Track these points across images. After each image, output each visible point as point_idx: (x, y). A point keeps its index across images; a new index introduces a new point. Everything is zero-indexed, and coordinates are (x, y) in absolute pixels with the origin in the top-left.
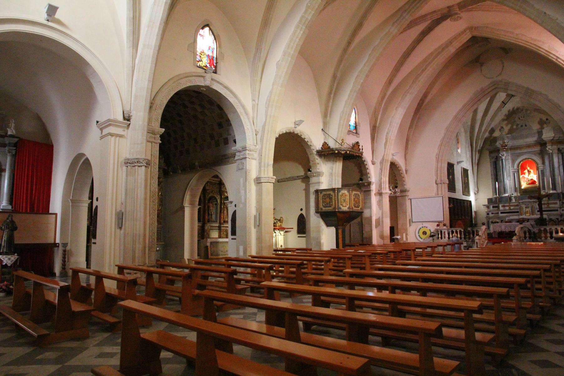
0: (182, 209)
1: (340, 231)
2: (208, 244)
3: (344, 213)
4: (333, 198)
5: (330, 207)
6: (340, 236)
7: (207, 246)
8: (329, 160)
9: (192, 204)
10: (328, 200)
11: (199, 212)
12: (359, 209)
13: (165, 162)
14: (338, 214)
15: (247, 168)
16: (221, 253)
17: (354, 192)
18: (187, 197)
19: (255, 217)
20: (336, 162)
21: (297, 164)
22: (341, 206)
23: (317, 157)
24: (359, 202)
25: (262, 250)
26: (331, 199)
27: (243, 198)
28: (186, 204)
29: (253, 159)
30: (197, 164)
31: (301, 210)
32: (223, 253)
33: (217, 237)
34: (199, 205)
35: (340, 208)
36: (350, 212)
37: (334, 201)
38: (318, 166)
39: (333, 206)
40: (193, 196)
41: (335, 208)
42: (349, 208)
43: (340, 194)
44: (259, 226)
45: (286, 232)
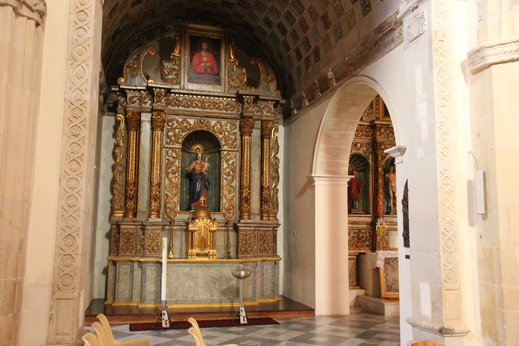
0: (310, 183)
2: (380, 264)
7: (377, 270)
9: (332, 171)
11: (349, 189)
13: (278, 88)
15: (435, 27)
18: (320, 158)
19: (471, 185)
25: (501, 304)
27: (424, 126)
28: (319, 170)
30: (330, 74)
34: (350, 173)
40: (333, 154)
44: (485, 216)
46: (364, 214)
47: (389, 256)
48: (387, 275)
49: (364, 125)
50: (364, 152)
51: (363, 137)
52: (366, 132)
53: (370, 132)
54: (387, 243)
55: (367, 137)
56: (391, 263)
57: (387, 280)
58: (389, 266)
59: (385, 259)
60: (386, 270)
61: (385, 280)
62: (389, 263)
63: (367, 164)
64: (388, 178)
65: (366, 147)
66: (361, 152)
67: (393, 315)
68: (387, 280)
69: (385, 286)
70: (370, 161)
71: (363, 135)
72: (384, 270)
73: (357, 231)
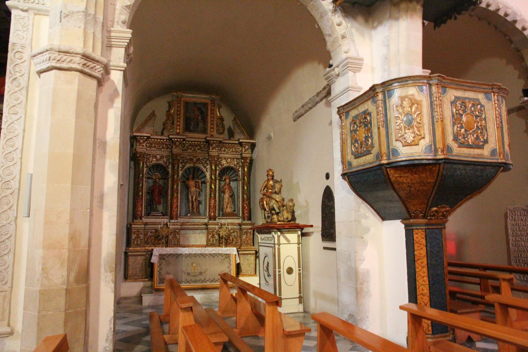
1: (419, 236)
3: (413, 167)
4: (374, 122)
5: (369, 153)
6: (421, 252)
8: (380, 23)
10: (362, 134)
12: (486, 152)
14: (393, 175)
16: (184, 277)
17: (452, 94)
20: (397, 19)
21: (316, 64)
22: (398, 145)
23: (338, 18)
24: (484, 128)
26: (367, 125)
29: (39, 12)
31: (327, 176)
32: (189, 278)
33: (205, 243)
35: (395, 152)
36: (436, 163)
37: (375, 130)
38: (345, 45)
39: (375, 151)
41: (379, 156)
42: (433, 147)
43: (395, 99)
45: (303, 235)
46: (163, 216)
47: (165, 253)
48: (161, 269)
49: (163, 139)
50: (164, 162)
51: (163, 150)
52: (166, 145)
53: (170, 145)
54: (178, 241)
55: (167, 149)
56: (166, 258)
57: (160, 273)
58: (164, 262)
59: (160, 255)
60: (160, 264)
61: (158, 273)
62: (164, 259)
63: (168, 172)
64: (188, 185)
65: (166, 157)
66: (161, 162)
67: (151, 304)
68: (160, 273)
69: (158, 277)
70: (170, 170)
71: (163, 148)
72: (158, 265)
73: (154, 231)
